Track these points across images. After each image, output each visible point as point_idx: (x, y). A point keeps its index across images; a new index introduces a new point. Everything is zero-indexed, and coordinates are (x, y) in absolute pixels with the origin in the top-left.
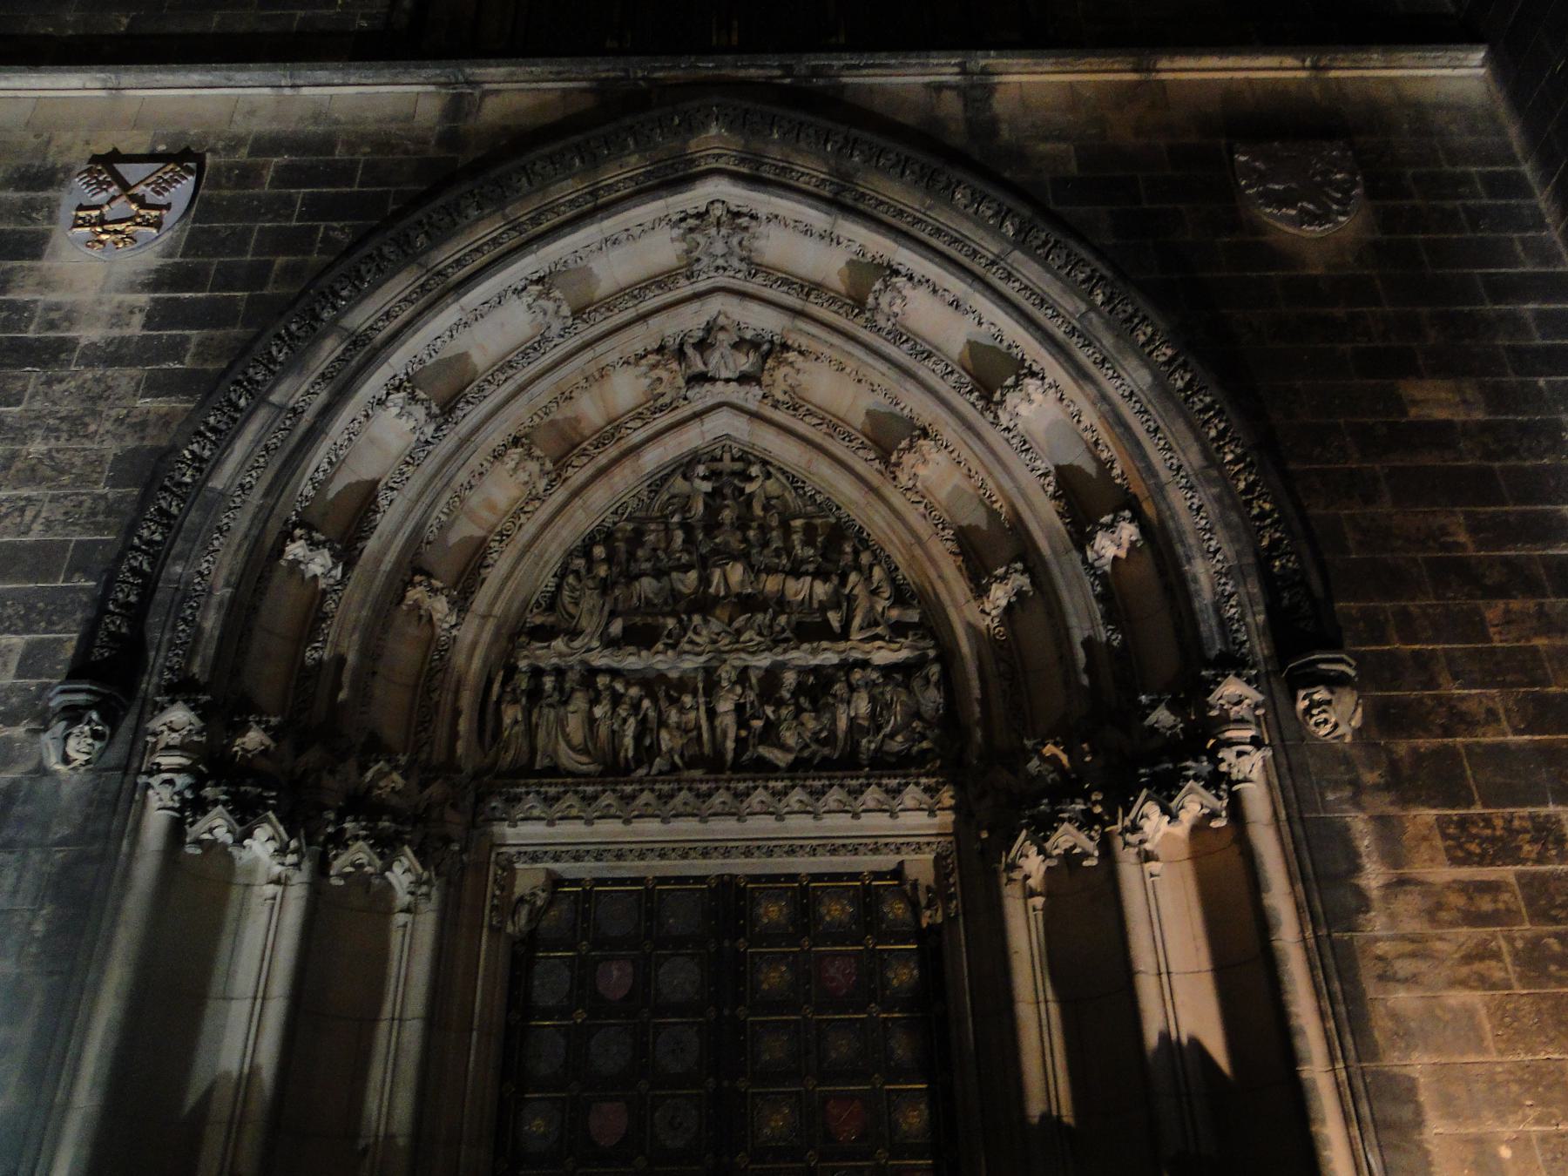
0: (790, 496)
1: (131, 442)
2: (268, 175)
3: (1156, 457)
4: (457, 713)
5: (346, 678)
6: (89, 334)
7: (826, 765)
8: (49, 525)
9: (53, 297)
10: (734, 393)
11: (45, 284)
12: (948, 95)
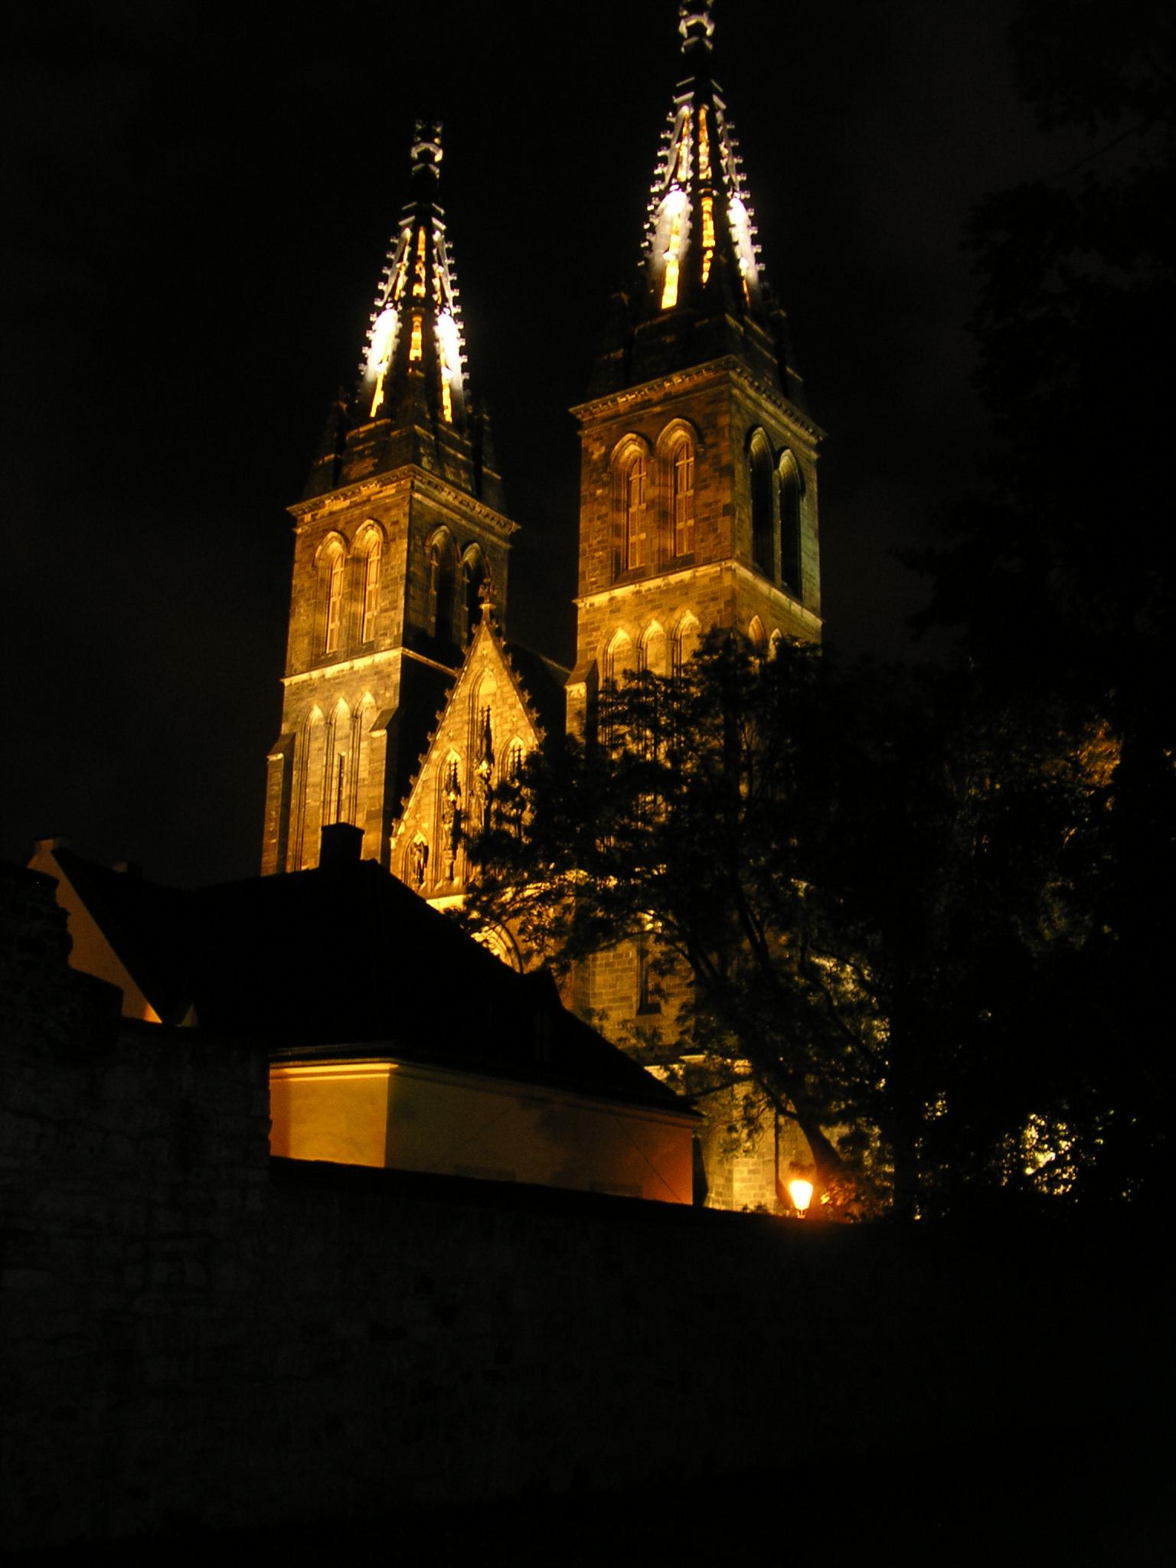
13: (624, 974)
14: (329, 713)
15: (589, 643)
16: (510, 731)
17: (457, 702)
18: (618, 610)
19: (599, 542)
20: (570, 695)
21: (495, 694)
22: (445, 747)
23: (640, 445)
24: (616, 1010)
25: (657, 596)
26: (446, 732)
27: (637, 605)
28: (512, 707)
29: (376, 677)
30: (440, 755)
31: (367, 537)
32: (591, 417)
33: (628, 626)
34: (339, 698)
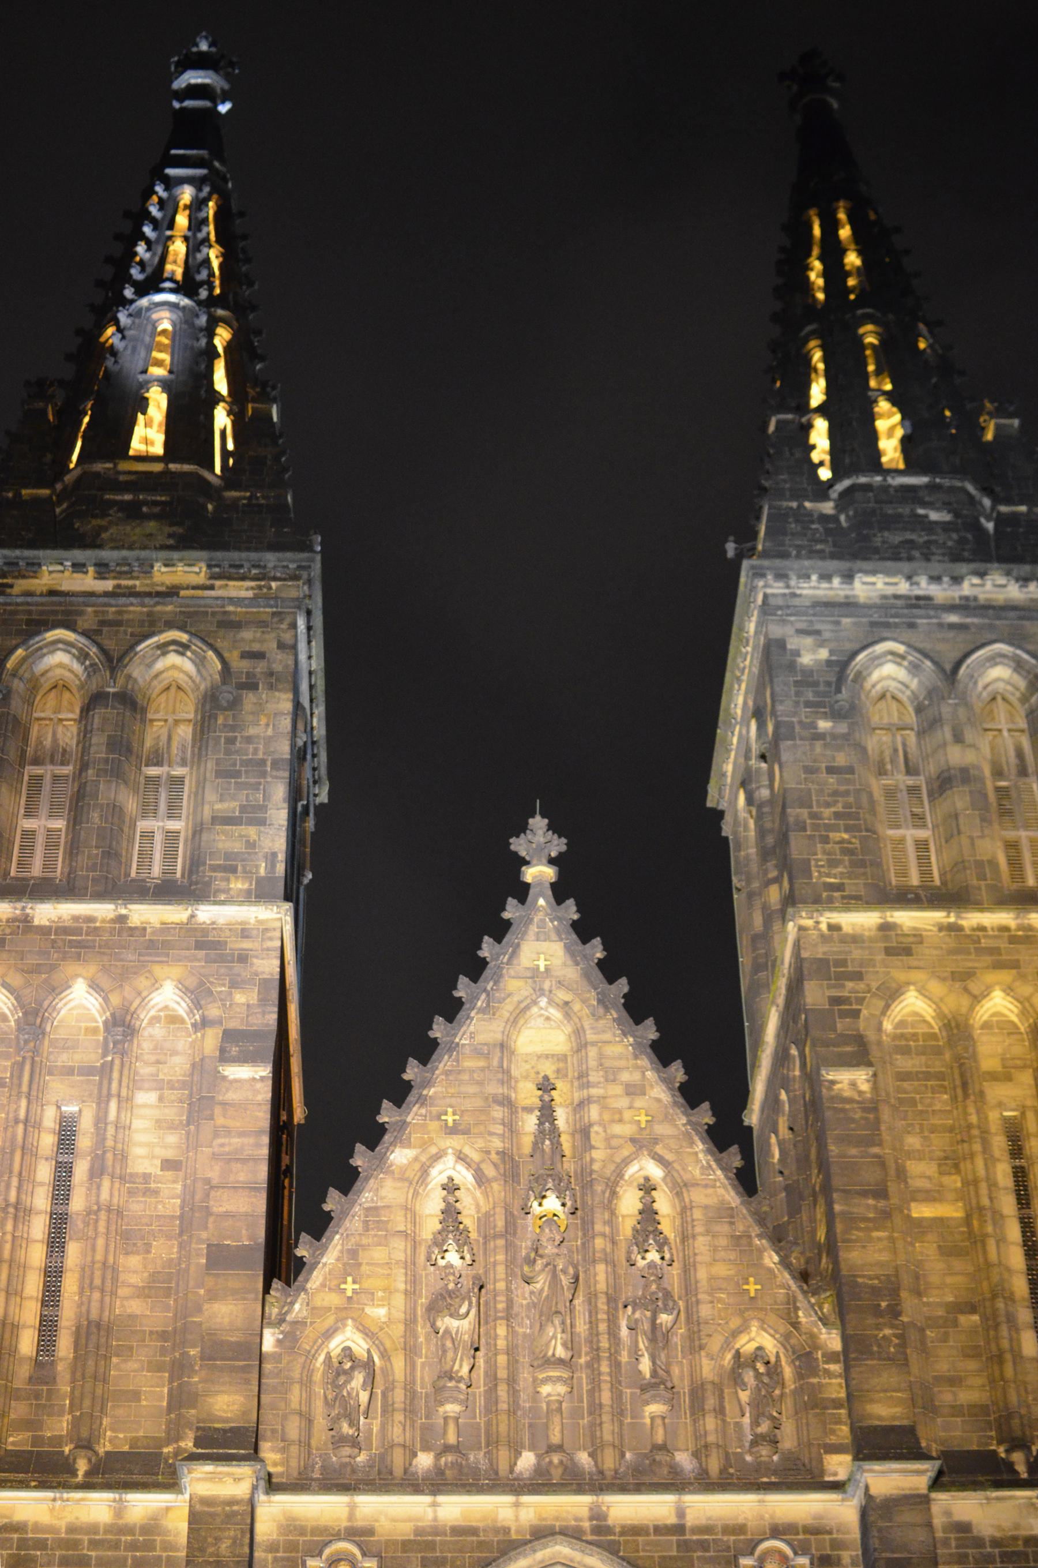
14: (41, 1005)
15: (836, 1001)
16: (633, 1140)
17: (467, 1050)
18: (907, 951)
19: (837, 815)
20: (830, 1089)
21: (563, 1058)
22: (431, 1142)
23: (914, 669)
25: (1003, 945)
28: (633, 1091)
29: (201, 954)
30: (416, 1159)
31: (160, 665)
32: (787, 591)
33: (936, 988)
34: (77, 976)
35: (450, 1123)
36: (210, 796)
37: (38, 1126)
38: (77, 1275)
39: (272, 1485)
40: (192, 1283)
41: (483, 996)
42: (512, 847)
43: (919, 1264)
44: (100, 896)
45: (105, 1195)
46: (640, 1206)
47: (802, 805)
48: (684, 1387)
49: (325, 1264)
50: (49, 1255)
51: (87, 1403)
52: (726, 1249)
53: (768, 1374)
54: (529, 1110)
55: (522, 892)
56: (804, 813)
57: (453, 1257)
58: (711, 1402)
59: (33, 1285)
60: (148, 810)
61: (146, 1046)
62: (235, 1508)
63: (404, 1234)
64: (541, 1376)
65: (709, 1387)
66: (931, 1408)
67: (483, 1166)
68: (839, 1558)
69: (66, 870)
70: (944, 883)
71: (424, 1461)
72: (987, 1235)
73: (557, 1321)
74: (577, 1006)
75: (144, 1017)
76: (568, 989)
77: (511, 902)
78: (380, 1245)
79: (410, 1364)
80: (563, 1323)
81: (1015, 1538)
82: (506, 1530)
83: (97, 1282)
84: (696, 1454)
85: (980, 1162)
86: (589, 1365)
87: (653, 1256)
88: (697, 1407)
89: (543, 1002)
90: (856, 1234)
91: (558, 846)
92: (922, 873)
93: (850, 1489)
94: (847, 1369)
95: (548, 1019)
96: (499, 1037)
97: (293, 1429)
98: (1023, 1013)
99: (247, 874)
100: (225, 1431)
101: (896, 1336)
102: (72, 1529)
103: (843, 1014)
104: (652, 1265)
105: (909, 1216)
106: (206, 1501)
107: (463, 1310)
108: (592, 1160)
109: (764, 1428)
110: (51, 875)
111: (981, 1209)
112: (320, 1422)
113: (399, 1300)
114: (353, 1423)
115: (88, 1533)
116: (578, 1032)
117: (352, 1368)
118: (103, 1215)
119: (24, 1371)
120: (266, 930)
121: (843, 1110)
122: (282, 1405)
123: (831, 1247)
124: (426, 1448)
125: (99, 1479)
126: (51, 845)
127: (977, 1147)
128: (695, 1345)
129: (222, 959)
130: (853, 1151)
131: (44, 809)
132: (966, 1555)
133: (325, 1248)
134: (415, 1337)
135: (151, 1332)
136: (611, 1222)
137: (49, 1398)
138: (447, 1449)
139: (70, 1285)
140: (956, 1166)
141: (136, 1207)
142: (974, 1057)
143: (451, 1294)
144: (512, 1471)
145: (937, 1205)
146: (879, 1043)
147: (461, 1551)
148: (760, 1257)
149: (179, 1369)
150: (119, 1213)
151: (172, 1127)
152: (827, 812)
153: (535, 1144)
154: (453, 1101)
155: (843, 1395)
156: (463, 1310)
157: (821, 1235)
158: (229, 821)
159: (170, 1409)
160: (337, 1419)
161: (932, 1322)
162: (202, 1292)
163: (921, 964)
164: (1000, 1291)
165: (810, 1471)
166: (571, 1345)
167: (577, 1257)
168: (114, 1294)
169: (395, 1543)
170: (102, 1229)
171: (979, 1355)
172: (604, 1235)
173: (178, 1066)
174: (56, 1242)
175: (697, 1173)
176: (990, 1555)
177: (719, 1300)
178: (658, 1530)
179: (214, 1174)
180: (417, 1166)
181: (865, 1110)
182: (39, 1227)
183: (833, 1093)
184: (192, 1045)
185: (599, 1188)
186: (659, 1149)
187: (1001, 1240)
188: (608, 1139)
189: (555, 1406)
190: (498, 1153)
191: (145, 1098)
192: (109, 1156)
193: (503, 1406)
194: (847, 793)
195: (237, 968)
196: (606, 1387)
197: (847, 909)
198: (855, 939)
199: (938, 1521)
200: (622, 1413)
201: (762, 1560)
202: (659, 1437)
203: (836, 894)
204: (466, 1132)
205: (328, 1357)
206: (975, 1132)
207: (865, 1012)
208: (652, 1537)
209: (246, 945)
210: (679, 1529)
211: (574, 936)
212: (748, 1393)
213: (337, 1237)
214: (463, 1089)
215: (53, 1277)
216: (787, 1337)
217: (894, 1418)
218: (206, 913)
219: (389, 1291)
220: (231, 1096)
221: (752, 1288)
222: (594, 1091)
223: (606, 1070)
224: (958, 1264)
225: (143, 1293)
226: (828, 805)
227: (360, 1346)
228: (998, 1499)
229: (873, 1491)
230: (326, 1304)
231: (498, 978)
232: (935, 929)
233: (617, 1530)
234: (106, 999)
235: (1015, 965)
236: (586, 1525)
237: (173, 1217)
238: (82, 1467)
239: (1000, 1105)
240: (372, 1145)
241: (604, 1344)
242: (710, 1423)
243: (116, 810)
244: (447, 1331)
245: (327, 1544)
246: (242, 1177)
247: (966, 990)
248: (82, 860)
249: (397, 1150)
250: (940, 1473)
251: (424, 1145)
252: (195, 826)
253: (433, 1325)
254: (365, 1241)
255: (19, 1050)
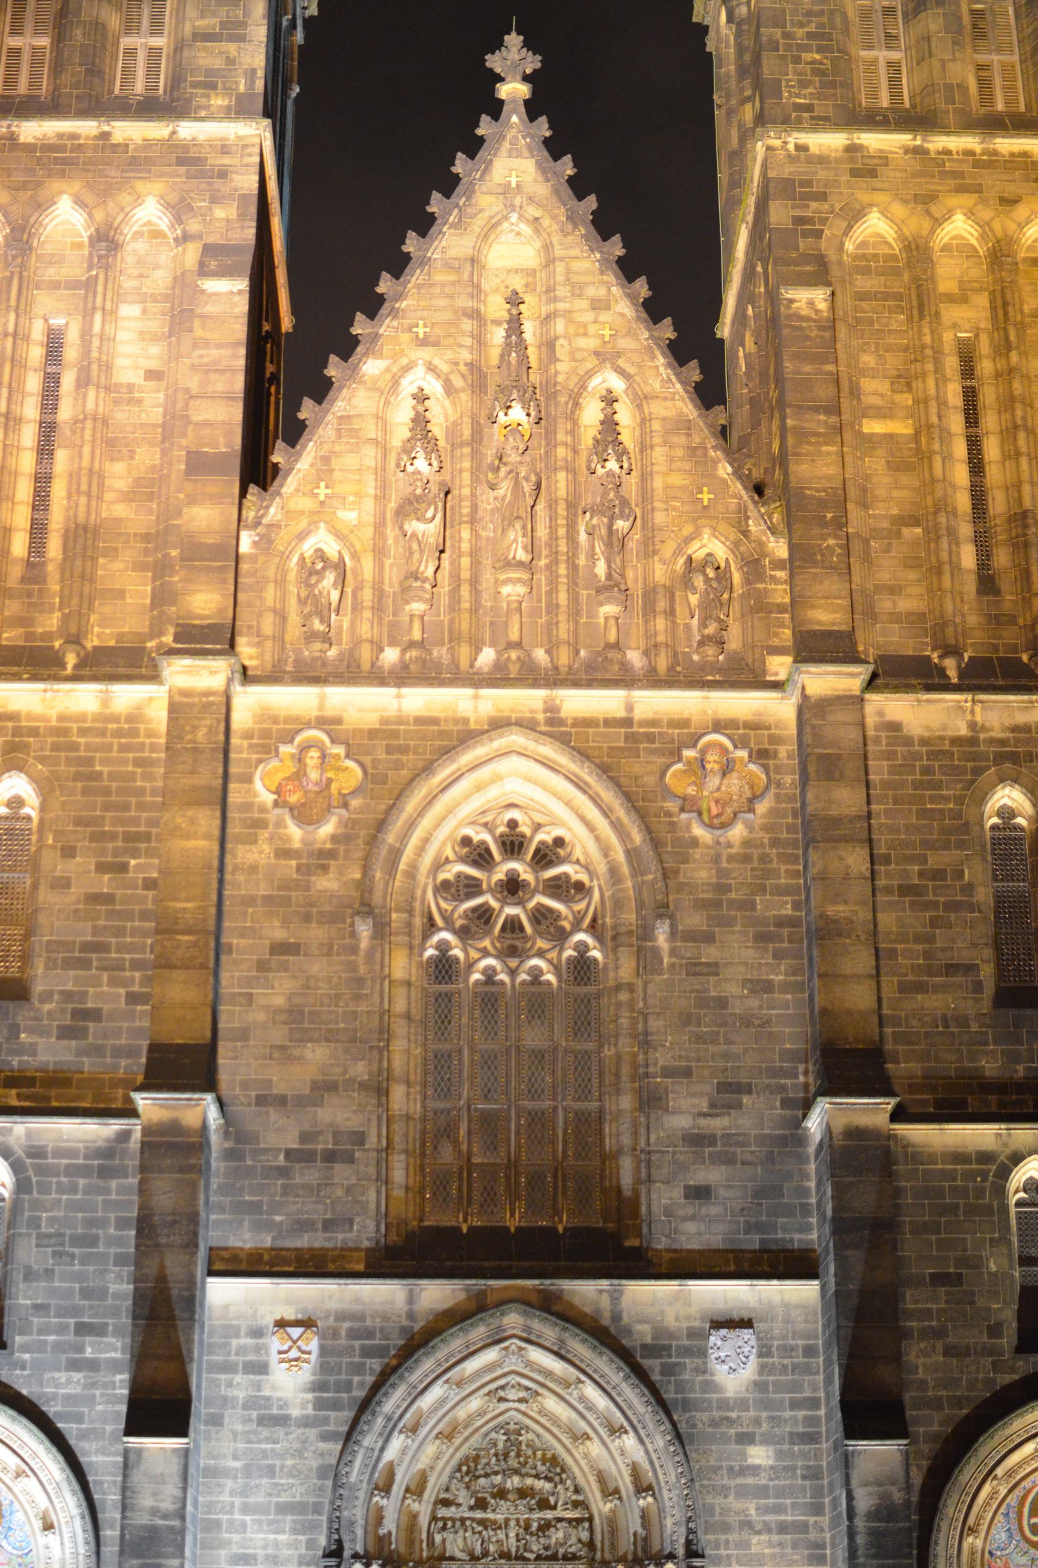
0: (536, 1440)
1: (320, 1461)
2: (343, 1333)
3: (661, 1477)
4: (421, 1542)
5: (393, 1539)
6: (295, 1412)
7: (548, 1558)
8: (301, 1494)
9: (278, 1394)
10: (516, 1405)
11: (274, 1388)
12: (605, 1295)
13: (953, 916)
14: (27, 221)
15: (799, 221)
16: (596, 354)
17: (439, 264)
18: (872, 173)
19: (810, 36)
20: (788, 307)
21: (533, 272)
22: (402, 353)
24: (935, 992)
25: (967, 168)
26: (406, 322)
27: (915, 175)
28: (598, 305)
30: (387, 370)
33: (899, 210)
34: (62, 192)
35: (421, 336)
36: (191, 12)
37: (27, 338)
38: (65, 481)
39: (246, 676)
40: (173, 488)
41: (456, 211)
42: (488, 64)
43: (867, 478)
44: (84, 113)
45: (90, 405)
46: (601, 417)
47: (776, 26)
48: (637, 590)
49: (299, 470)
50: (39, 462)
51: (75, 601)
52: (682, 459)
53: (718, 579)
54: (497, 323)
55: (496, 109)
56: (778, 33)
57: (421, 464)
58: (662, 604)
59: (24, 491)
60: (131, 27)
61: (130, 260)
62: (211, 699)
63: (375, 441)
64: (502, 577)
65: (661, 590)
66: (872, 615)
67: (452, 377)
68: (776, 752)
69: (51, 88)
70: (913, 106)
71: (391, 656)
72: (934, 452)
73: (518, 525)
74: (546, 222)
75: (128, 231)
76: (539, 205)
77: (485, 119)
78: (351, 451)
79: (379, 565)
80: (524, 527)
81: (942, 738)
82: (466, 721)
83: (84, 487)
84: (646, 653)
85: (931, 382)
86: (548, 567)
87: (612, 465)
88: (649, 610)
89: (514, 217)
90: (806, 448)
91: (532, 63)
92: (892, 95)
93: (788, 688)
94: (792, 576)
95: (518, 234)
96: (470, 252)
97: (268, 624)
98: (983, 237)
99: (228, 90)
100: (202, 627)
101: (839, 546)
102: (62, 718)
103: (806, 234)
104: (610, 474)
105: (860, 432)
106: (184, 693)
107: (429, 514)
108: (557, 373)
109: (711, 629)
110: (36, 92)
111: (929, 426)
112: (294, 619)
113: (369, 505)
114: (326, 620)
115: (76, 721)
116: (547, 247)
117: (324, 569)
118: (89, 424)
119: (16, 572)
120: (245, 146)
121: (801, 328)
122: (258, 602)
123: (782, 460)
124: (392, 643)
125: (86, 672)
126: (36, 63)
127: (930, 367)
128: (649, 550)
129: (202, 175)
130: (808, 368)
131: (29, 27)
132: (895, 753)
133: (299, 455)
134: (383, 537)
135: (135, 535)
136: (573, 432)
137: (40, 597)
138: (412, 644)
139: (58, 490)
140: (909, 385)
141: (121, 416)
142: (933, 279)
143: (418, 499)
144: (472, 666)
145: (889, 422)
146: (840, 263)
147: (422, 739)
148: (715, 468)
149: (161, 569)
150: (105, 422)
151: (155, 338)
152: (800, 32)
153: (502, 356)
154: (424, 314)
155: (787, 600)
156: (429, 514)
157: (776, 447)
158: (209, 37)
159: (153, 606)
160: (308, 617)
161: (877, 533)
162: (182, 496)
163: (885, 186)
164: (943, 506)
165: (752, 671)
166: (532, 548)
167: (540, 466)
168: (100, 498)
169: (361, 731)
170: (88, 435)
171: (920, 566)
172: (566, 444)
173: (161, 279)
174: (45, 450)
175: (657, 386)
176: (917, 753)
177: (674, 508)
178: (608, 722)
179: (193, 383)
180: (388, 376)
181: (821, 328)
182: (29, 436)
183: (791, 312)
184: (174, 258)
185: (562, 399)
186: (621, 362)
187: (948, 457)
188: (572, 353)
189: (515, 605)
190: (466, 364)
191: (129, 310)
192: (95, 367)
193: (465, 605)
194: (821, 13)
195: (218, 183)
196: (563, 589)
197: (814, 129)
198: (822, 160)
199: (871, 721)
200: (577, 613)
201: (703, 752)
202: (612, 637)
203: (805, 115)
204: (436, 344)
205: (302, 558)
206: (929, 352)
207: (827, 232)
208: (602, 729)
209: (226, 160)
210: (627, 722)
211: (546, 153)
212: (697, 596)
213: (311, 444)
214: (434, 302)
215: (42, 482)
216: (737, 544)
217: (833, 624)
218: (187, 130)
219: (359, 495)
220: (210, 309)
221: (706, 497)
222: (560, 306)
223: (573, 285)
224: (905, 479)
225: (127, 497)
226: (802, 25)
227: (332, 548)
228: (928, 701)
229: (809, 691)
230: (300, 507)
231: (470, 193)
232: (901, 151)
233: (570, 722)
234: (90, 215)
235: (978, 189)
236: (541, 717)
237: (155, 426)
238: (71, 660)
239: (955, 326)
240: (345, 356)
241: (563, 547)
242: (660, 624)
243: (99, 28)
244: (414, 535)
245: (298, 731)
246: (220, 387)
247: (928, 212)
248: (66, 78)
249: (370, 361)
250: (874, 676)
251: (395, 356)
252: (176, 43)
253: (401, 527)
254: (337, 448)
255: (7, 265)
